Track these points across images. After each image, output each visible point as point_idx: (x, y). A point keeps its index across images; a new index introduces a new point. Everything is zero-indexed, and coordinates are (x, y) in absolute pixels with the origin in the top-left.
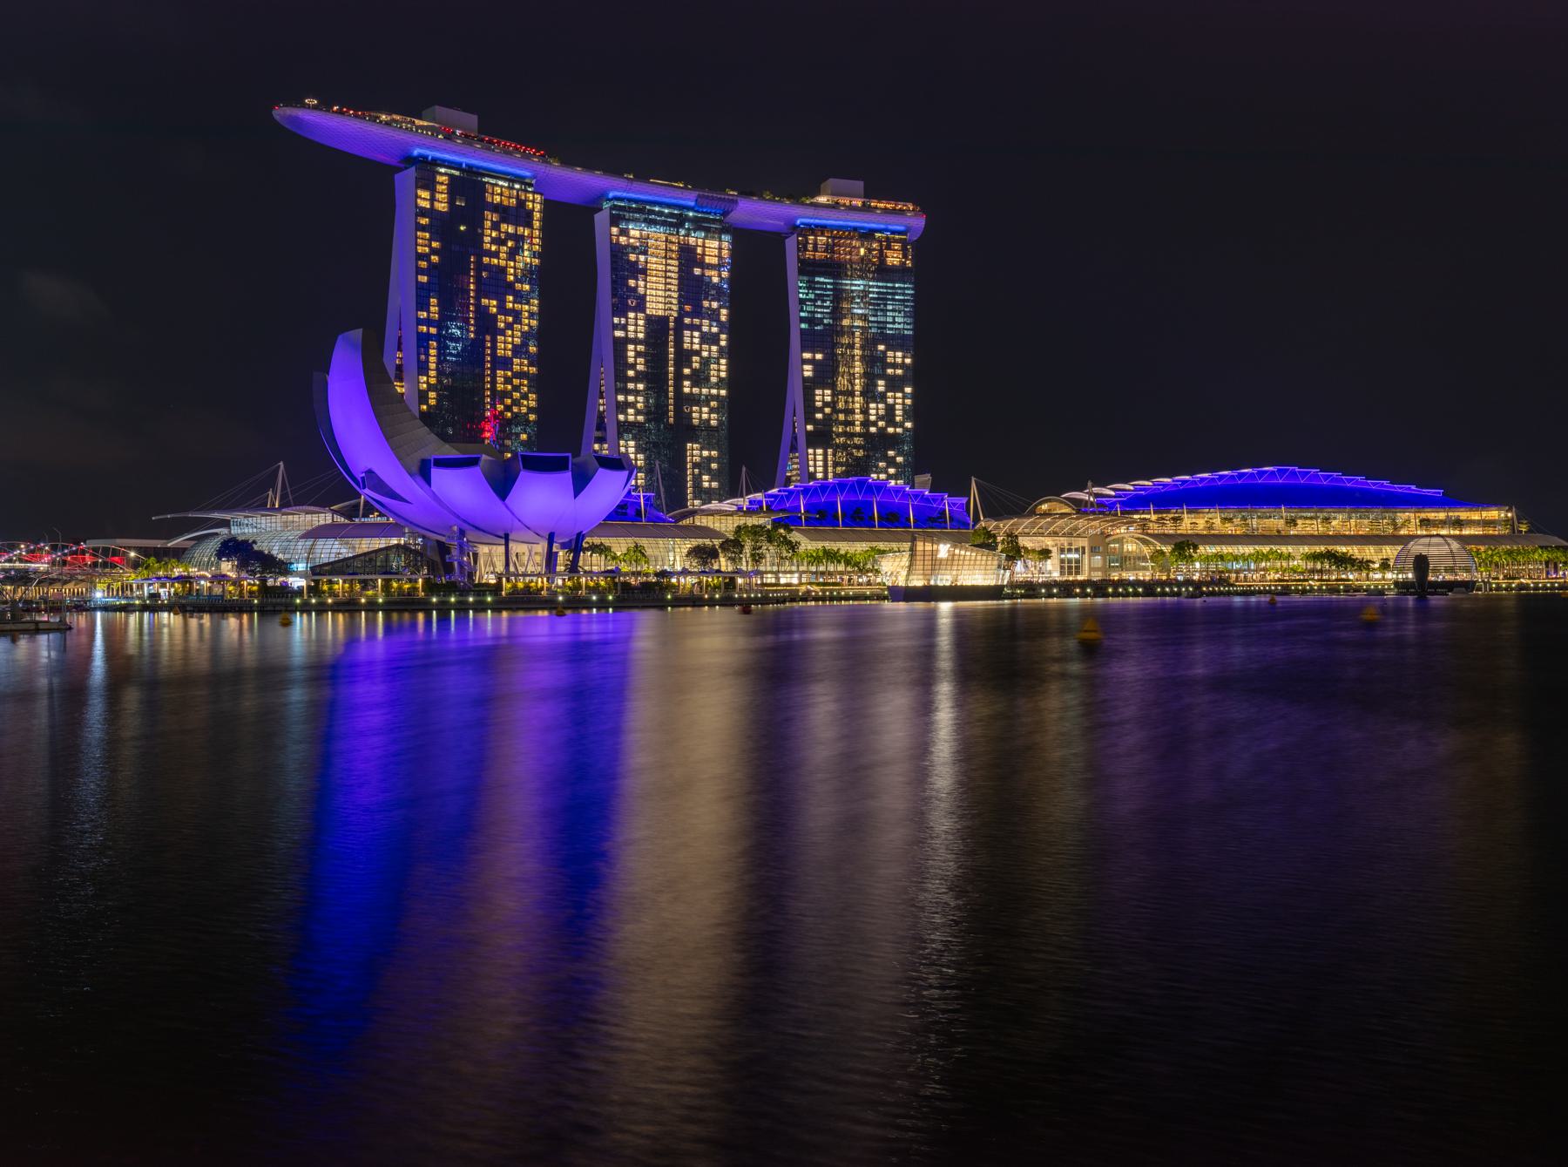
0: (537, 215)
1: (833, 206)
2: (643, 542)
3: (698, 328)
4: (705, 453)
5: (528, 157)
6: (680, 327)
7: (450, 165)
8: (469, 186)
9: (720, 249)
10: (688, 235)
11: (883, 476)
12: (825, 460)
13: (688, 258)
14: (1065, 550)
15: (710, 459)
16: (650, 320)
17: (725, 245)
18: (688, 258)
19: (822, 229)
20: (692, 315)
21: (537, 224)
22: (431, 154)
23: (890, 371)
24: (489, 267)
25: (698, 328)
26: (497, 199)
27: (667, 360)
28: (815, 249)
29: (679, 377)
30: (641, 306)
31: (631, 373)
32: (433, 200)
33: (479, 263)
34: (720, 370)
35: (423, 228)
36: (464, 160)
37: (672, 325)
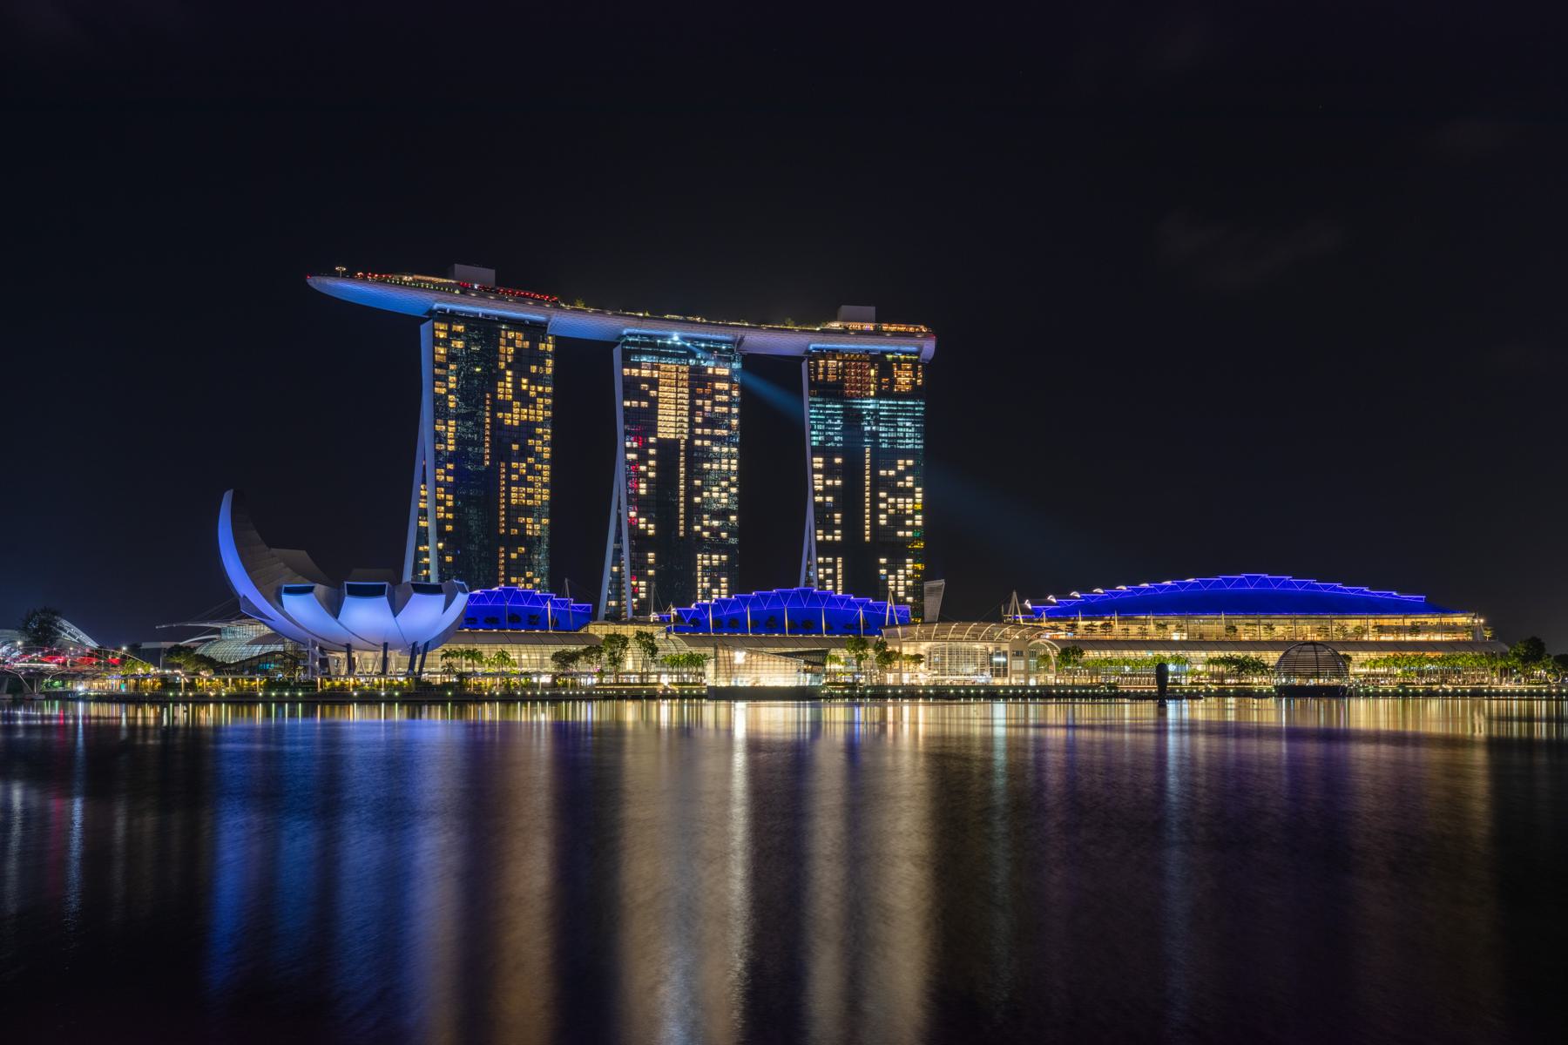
1: (847, 336)
2: (507, 648)
19: (834, 353)
27: (678, 478)
28: (826, 373)
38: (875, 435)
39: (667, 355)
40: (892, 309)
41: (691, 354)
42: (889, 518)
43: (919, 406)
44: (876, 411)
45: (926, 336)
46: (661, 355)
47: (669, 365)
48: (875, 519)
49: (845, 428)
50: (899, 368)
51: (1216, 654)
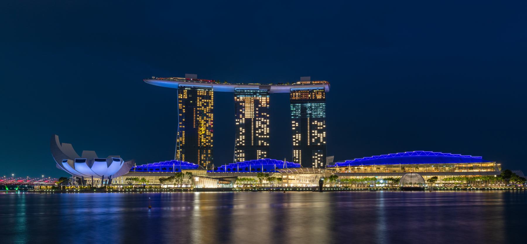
0: (212, 97)
3: (260, 120)
4: (263, 153)
5: (209, 83)
6: (255, 120)
7: (188, 87)
8: (193, 92)
9: (266, 99)
10: (256, 97)
11: (319, 155)
12: (299, 153)
13: (257, 103)
14: (376, 178)
15: (264, 154)
16: (246, 119)
17: (268, 98)
18: (257, 103)
19: (298, 91)
20: (258, 117)
21: (212, 99)
22: (183, 85)
23: (319, 128)
24: (199, 110)
25: (260, 120)
26: (201, 94)
29: (255, 133)
30: (244, 115)
31: (241, 133)
32: (183, 96)
33: (196, 110)
34: (267, 130)
35: (180, 103)
36: (192, 86)
37: (252, 120)
38: (311, 114)
39: (247, 95)
40: (314, 77)
41: (255, 93)
42: (315, 140)
43: (323, 105)
44: (311, 107)
45: (326, 84)
46: (245, 95)
47: (248, 97)
48: (311, 140)
49: (301, 112)
50: (317, 94)
51: (386, 177)
